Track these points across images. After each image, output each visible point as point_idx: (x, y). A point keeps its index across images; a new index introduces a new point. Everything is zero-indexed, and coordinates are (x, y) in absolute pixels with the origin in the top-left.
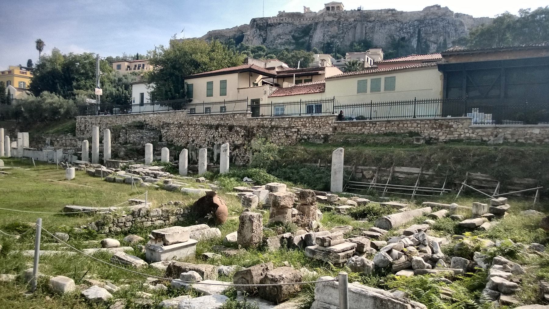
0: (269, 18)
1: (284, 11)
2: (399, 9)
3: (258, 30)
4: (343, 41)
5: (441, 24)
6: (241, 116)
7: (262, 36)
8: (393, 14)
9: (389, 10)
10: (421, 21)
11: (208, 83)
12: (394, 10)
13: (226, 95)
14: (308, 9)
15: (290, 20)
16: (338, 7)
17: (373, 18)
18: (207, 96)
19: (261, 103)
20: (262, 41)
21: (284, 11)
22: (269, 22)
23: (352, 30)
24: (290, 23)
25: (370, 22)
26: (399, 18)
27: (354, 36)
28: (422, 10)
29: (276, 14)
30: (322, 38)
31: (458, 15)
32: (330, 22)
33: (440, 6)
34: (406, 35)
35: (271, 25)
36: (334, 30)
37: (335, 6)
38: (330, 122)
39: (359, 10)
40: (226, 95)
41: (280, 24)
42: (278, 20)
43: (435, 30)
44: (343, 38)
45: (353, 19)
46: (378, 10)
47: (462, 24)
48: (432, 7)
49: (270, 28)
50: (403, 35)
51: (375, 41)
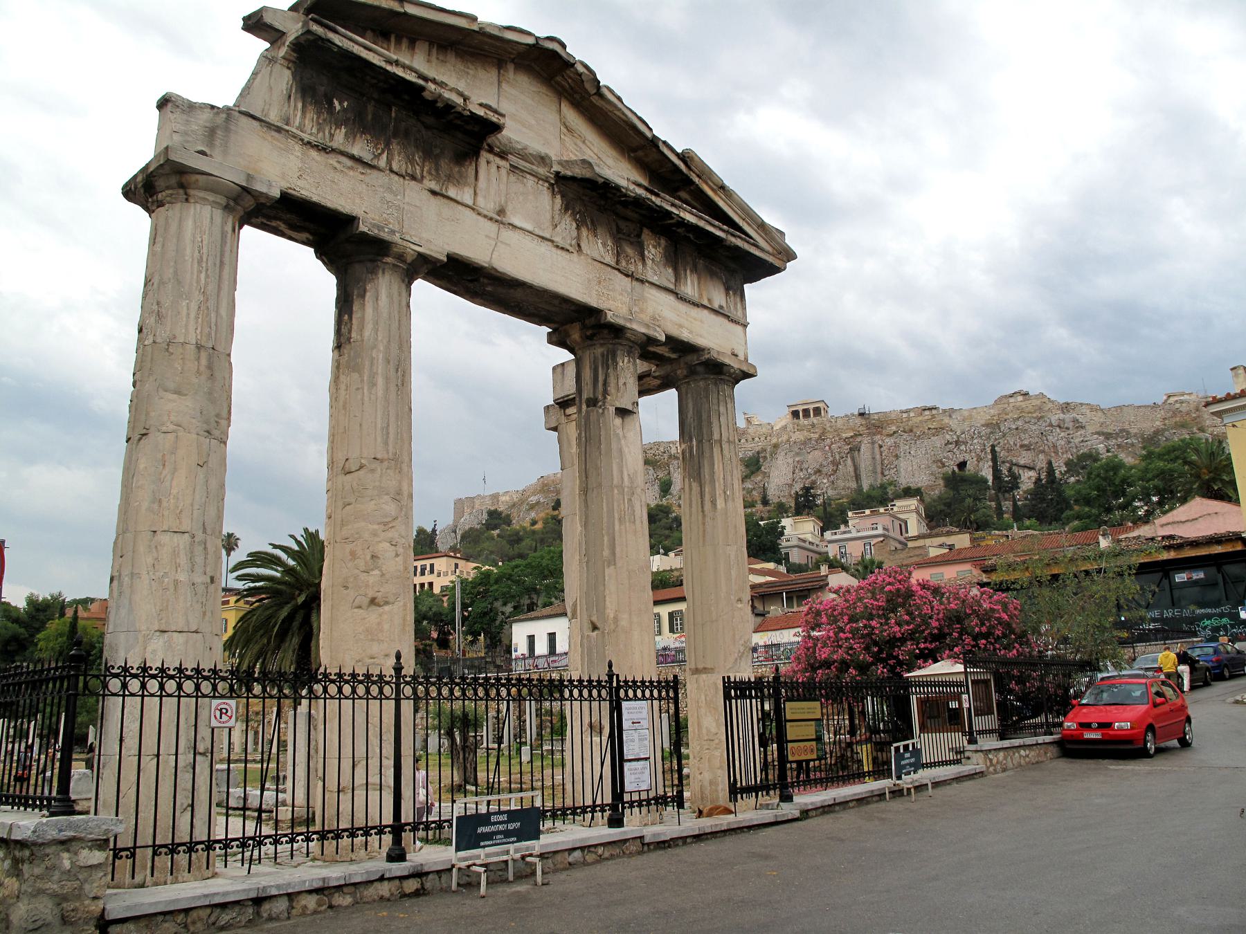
10: (993, 426)
17: (894, 428)
32: (804, 443)
34: (967, 457)
36: (814, 458)
43: (1026, 442)
46: (902, 412)
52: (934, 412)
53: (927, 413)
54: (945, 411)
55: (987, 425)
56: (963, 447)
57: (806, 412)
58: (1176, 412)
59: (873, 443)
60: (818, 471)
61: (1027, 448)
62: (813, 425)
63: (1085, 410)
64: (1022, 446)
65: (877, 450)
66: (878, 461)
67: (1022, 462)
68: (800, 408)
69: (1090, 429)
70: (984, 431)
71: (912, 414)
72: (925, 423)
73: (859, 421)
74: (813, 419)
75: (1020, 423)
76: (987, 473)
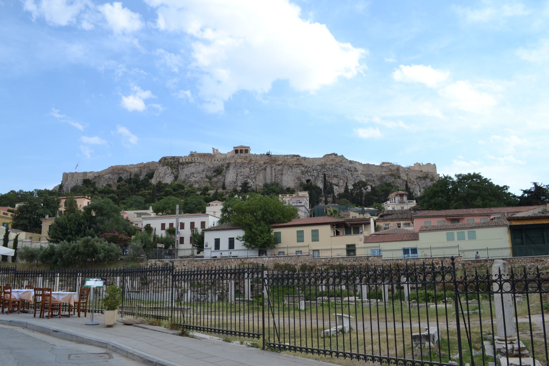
0: (181, 157)
1: (196, 152)
2: (302, 155)
3: (170, 168)
4: (256, 181)
5: (340, 169)
6: (376, 258)
7: (173, 173)
8: (298, 159)
9: (294, 156)
10: (323, 166)
11: (298, 232)
12: (298, 156)
13: (318, 241)
14: (217, 150)
15: (202, 161)
16: (247, 151)
17: (281, 162)
18: (298, 241)
19: (357, 246)
20: (173, 178)
21: (196, 152)
22: (181, 161)
23: (263, 171)
24: (202, 163)
25: (279, 165)
26: (303, 162)
27: (265, 178)
28: (322, 157)
29: (187, 154)
30: (235, 177)
31: (351, 162)
33: (336, 155)
34: (311, 178)
35: (182, 164)
36: (246, 171)
37: (244, 149)
38: (459, 260)
39: (268, 155)
40: (318, 241)
41: (191, 163)
42: (190, 159)
43: (336, 174)
44: (255, 178)
45: (263, 162)
46: (285, 156)
47: (356, 170)
48: (330, 155)
49: (181, 166)
50: (308, 178)
51: (284, 182)
52: (298, 157)
53: (295, 157)
54: (303, 158)
55: (319, 165)
56: (309, 174)
57: (241, 151)
58: (390, 170)
59: (272, 167)
60: (248, 177)
61: (336, 176)
62: (247, 157)
63: (357, 164)
64: (334, 176)
65: (273, 171)
66: (274, 175)
67: (334, 182)
68: (239, 149)
69: (360, 172)
70: (318, 167)
71: (289, 157)
72: (297, 161)
73: (267, 157)
74: (243, 155)
75: (333, 166)
76: (320, 185)
